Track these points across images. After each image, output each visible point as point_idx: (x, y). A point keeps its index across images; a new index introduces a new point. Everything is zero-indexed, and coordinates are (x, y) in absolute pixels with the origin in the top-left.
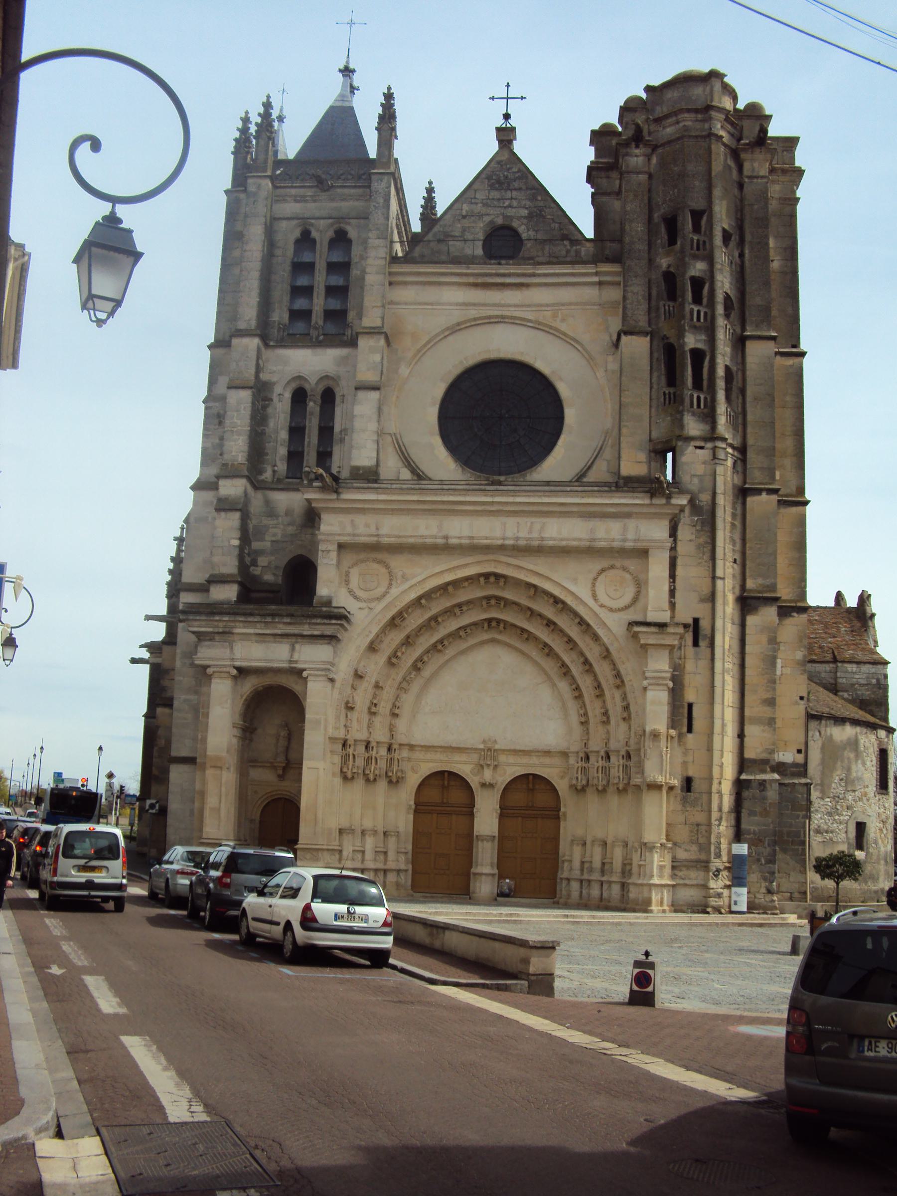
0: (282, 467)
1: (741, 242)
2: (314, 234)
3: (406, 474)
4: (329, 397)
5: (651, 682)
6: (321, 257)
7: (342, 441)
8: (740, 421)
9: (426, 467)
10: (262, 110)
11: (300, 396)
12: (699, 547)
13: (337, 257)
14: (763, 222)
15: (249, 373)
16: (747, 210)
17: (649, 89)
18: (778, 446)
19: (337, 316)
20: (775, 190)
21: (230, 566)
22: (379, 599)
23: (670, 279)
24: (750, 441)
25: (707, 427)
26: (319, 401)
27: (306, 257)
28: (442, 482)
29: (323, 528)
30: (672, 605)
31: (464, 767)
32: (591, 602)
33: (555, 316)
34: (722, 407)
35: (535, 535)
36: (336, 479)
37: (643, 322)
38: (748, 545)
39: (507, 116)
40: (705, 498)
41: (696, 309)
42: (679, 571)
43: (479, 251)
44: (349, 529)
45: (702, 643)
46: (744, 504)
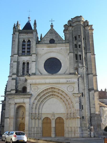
0: (22, 74)
1: (86, 39)
2: (25, 40)
3: (39, 74)
4: (28, 63)
6: (26, 44)
7: (30, 69)
8: (87, 64)
9: (42, 73)
10: (17, 23)
11: (24, 63)
12: (82, 82)
13: (29, 44)
14: (89, 37)
15: (16, 60)
16: (86, 35)
17: (72, 19)
18: (92, 68)
19: (29, 52)
20: (90, 32)
21: (14, 88)
22: (36, 92)
23: (76, 45)
24: (88, 67)
25: (82, 65)
26: (27, 64)
27: (24, 44)
28: (45, 74)
29: (28, 82)
30: (79, 91)
31: (49, 116)
32: (67, 91)
33: (60, 51)
34: (84, 63)
35: (59, 81)
36: (29, 74)
37: (72, 51)
38: (89, 82)
39: (52, 24)
40: (83, 75)
41: (80, 49)
42: (79, 86)
43: (49, 43)
44: (32, 82)
45: (83, 96)
46: (88, 76)
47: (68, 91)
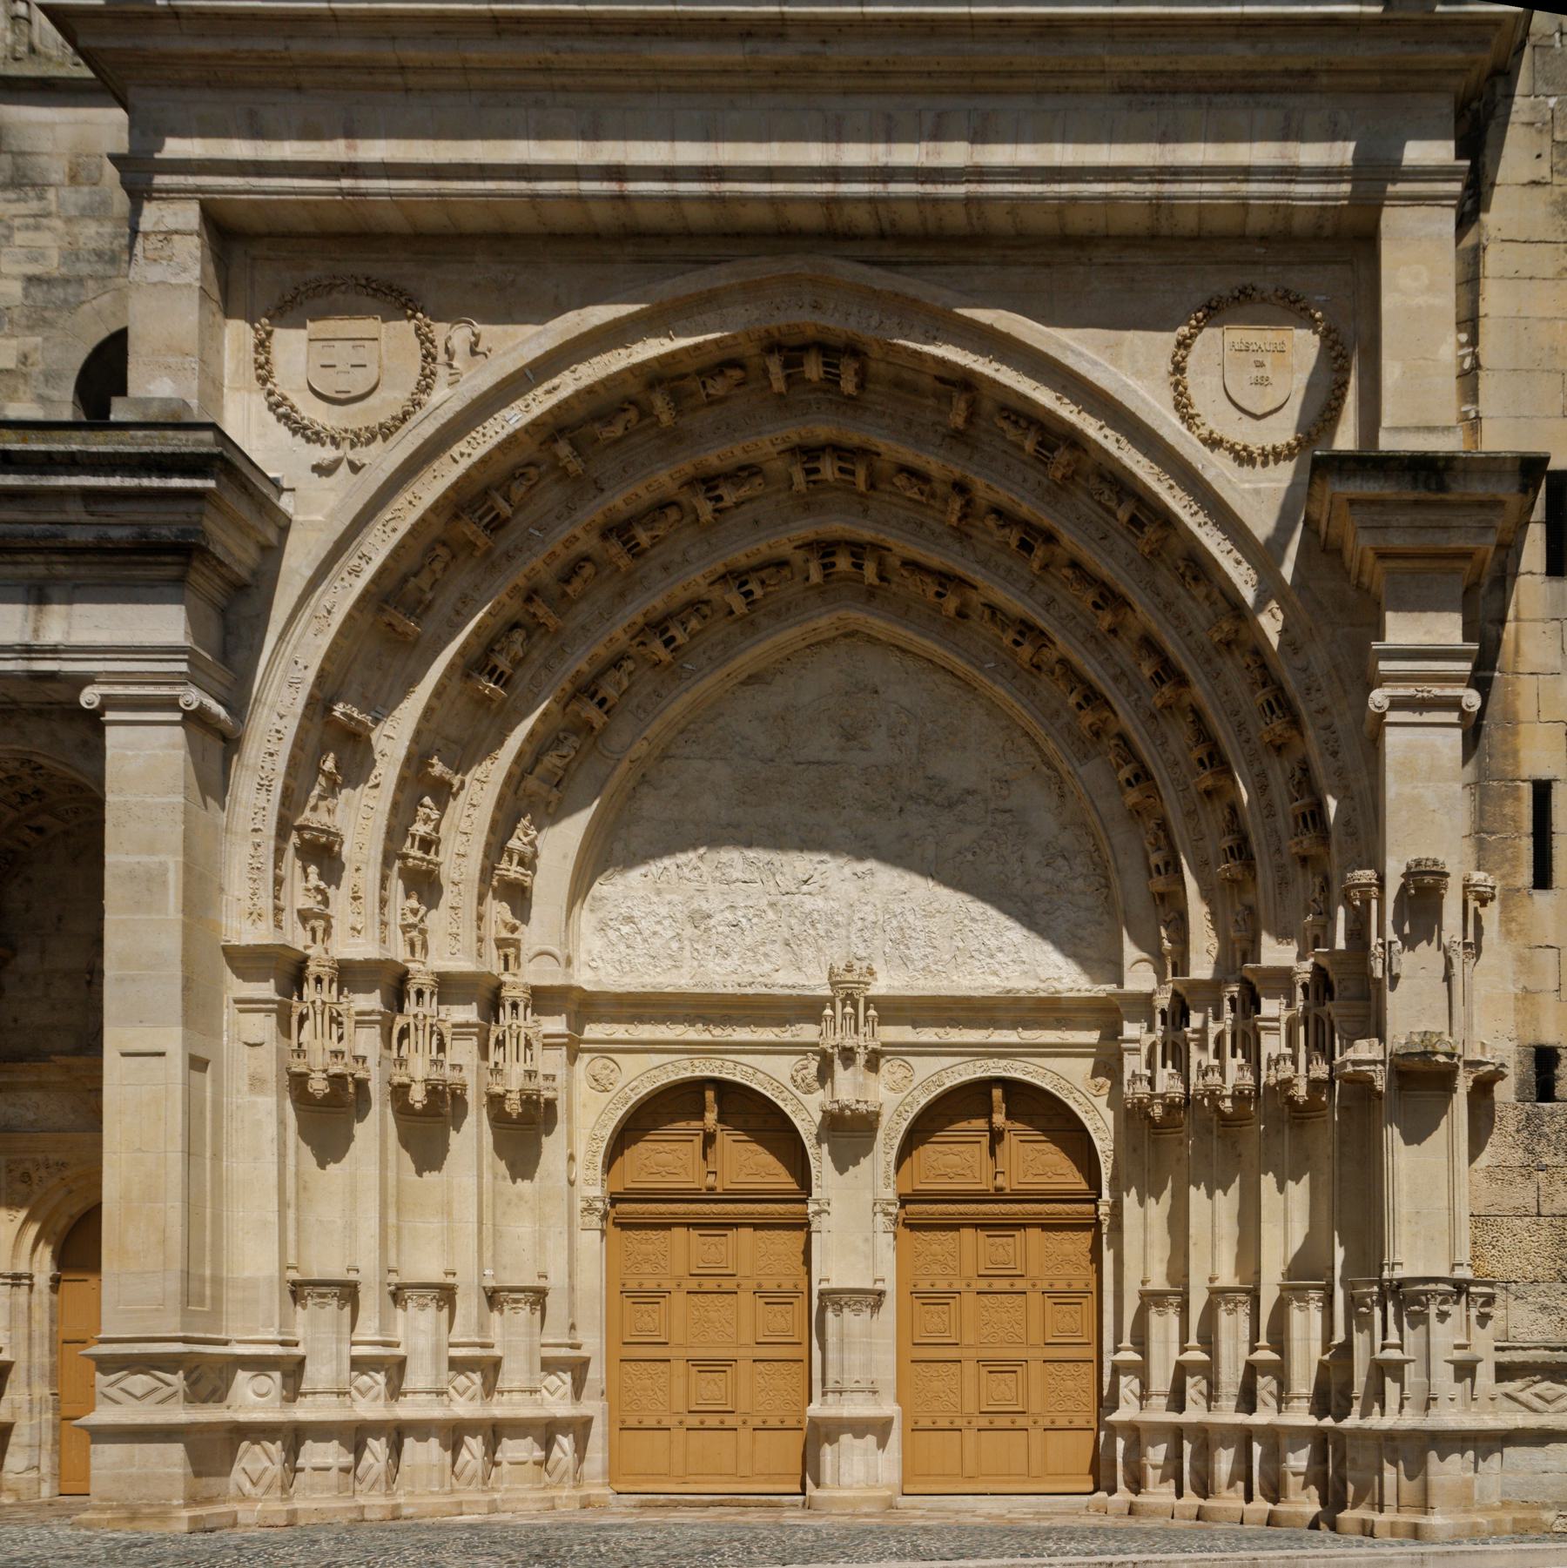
5: (1403, 691)
47: (1188, 419)
